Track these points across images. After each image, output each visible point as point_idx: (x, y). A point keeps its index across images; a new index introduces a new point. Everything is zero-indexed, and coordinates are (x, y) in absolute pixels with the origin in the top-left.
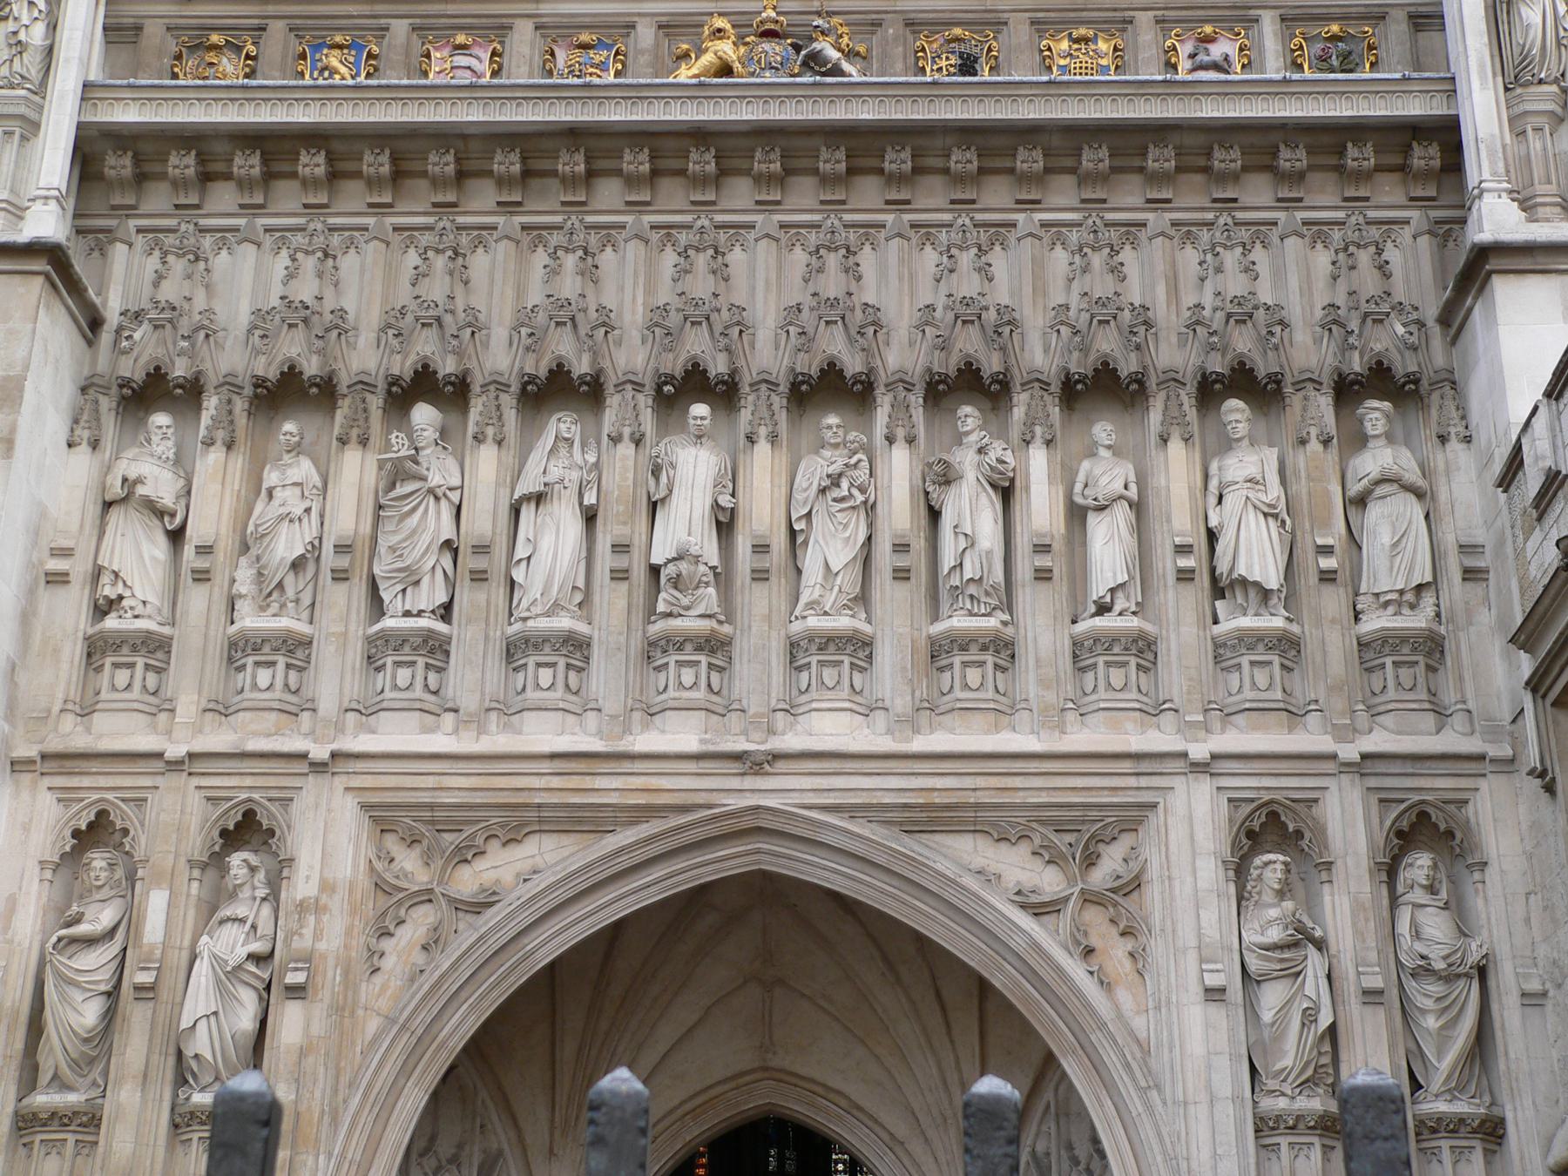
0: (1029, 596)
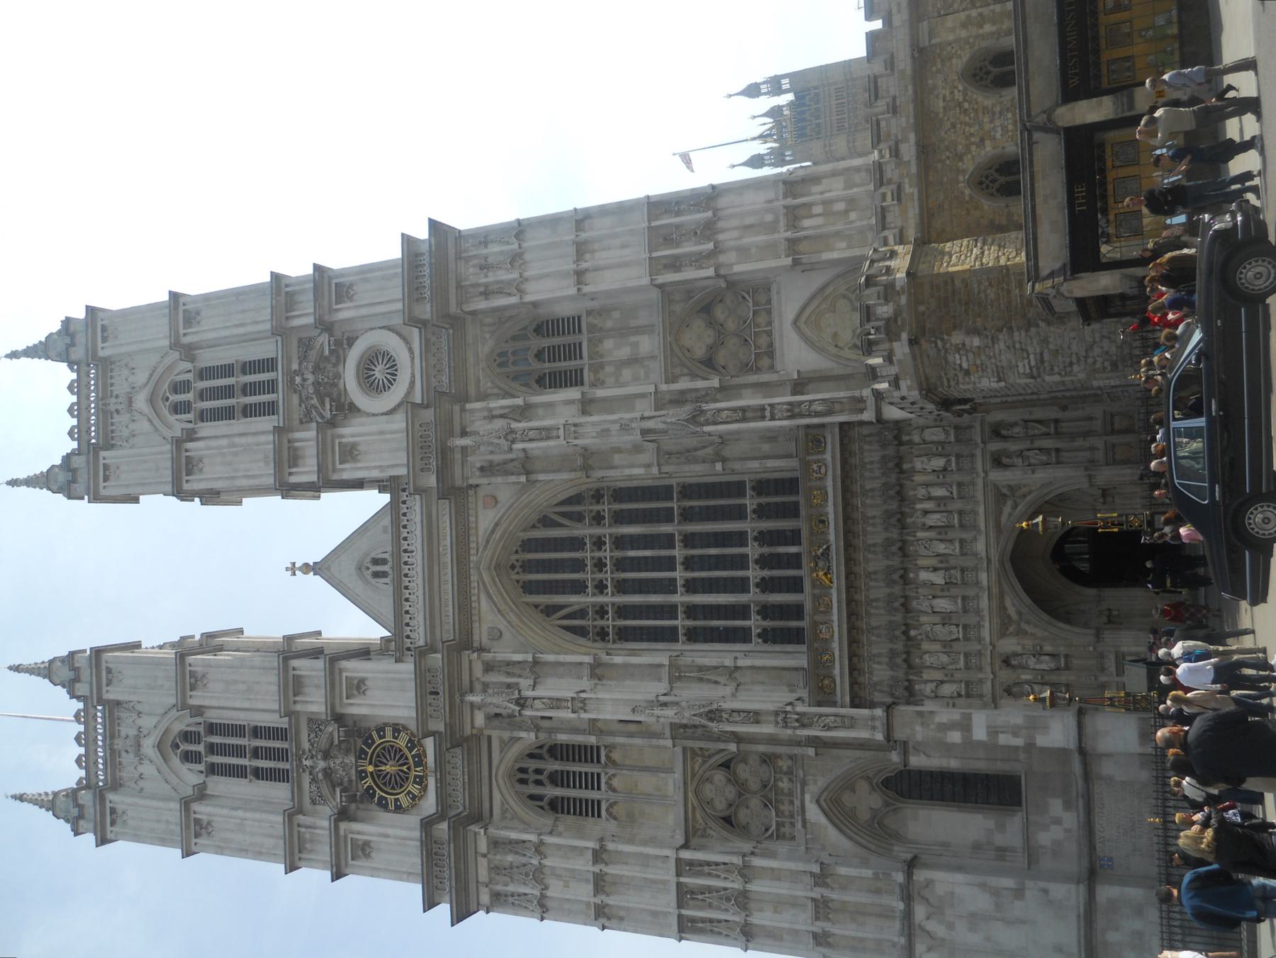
0: (949, 508)
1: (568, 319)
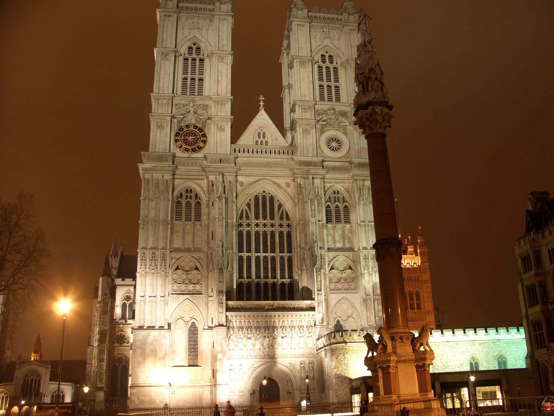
1: (349, 218)
